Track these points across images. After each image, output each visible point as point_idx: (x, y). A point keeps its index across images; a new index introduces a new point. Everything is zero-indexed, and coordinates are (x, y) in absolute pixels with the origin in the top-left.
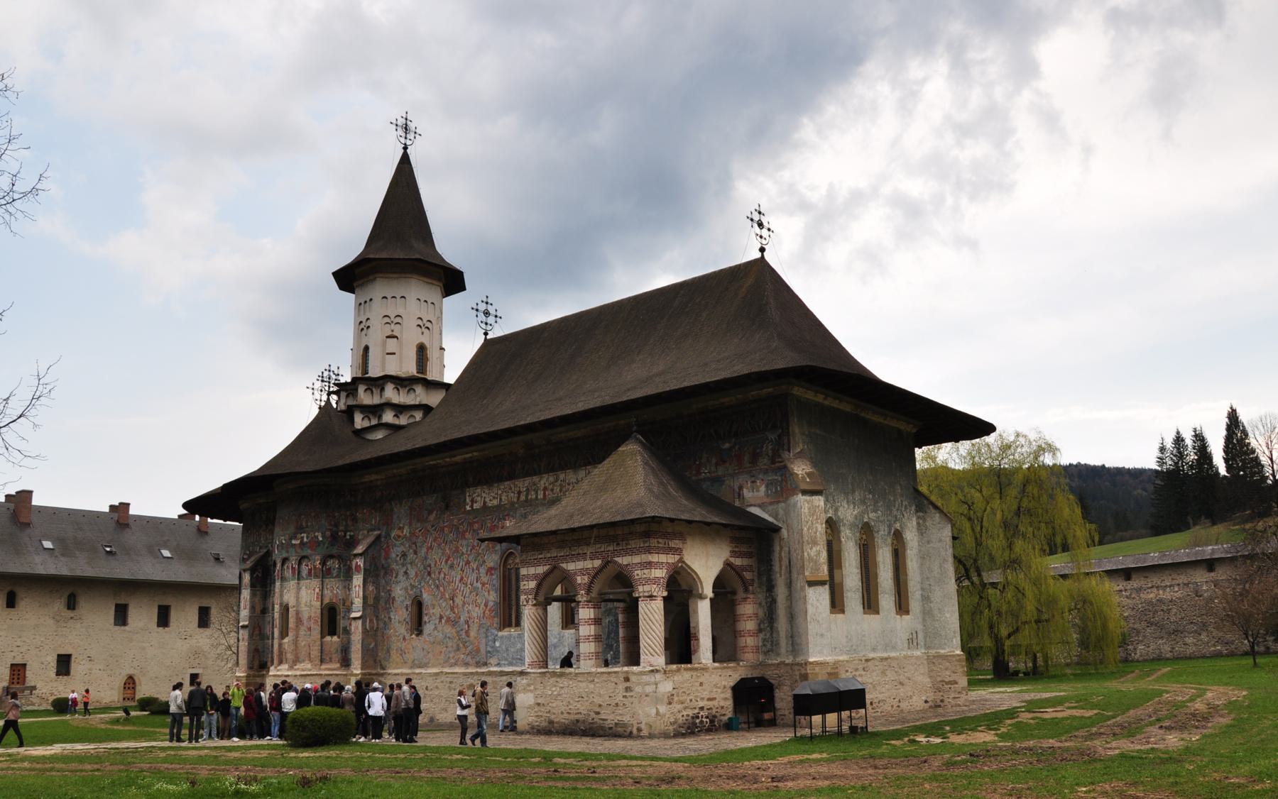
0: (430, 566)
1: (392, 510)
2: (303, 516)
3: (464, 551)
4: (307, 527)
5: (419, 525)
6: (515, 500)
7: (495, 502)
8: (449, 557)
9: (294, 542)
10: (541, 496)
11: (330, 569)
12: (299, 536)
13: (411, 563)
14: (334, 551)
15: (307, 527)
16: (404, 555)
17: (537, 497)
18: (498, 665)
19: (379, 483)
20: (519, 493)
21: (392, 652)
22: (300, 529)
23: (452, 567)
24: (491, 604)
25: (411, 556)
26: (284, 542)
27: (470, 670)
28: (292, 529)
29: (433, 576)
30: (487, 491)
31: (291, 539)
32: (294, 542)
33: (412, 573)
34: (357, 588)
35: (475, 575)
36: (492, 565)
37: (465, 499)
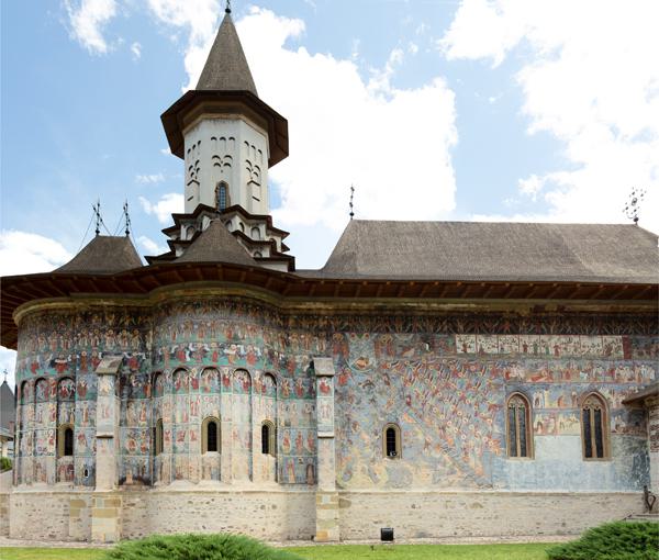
0: (410, 397)
1: (345, 340)
2: (237, 327)
3: (458, 387)
4: (243, 338)
5: (390, 358)
6: (522, 349)
7: (495, 351)
8: (437, 392)
9: (226, 351)
10: (552, 351)
11: (264, 387)
12: (233, 346)
13: (381, 393)
14: (272, 369)
15: (243, 338)
16: (370, 384)
17: (548, 353)
18: (506, 487)
19: (323, 312)
20: (525, 347)
21: (354, 474)
22: (234, 339)
23: (441, 400)
24: (495, 437)
25: (380, 385)
26: (208, 349)
27: (470, 491)
28: (222, 337)
29: (413, 405)
30: (483, 339)
31: (222, 347)
32: (226, 351)
33: (382, 401)
34: (325, 409)
35: (474, 409)
36: (495, 402)
37: (454, 344)
